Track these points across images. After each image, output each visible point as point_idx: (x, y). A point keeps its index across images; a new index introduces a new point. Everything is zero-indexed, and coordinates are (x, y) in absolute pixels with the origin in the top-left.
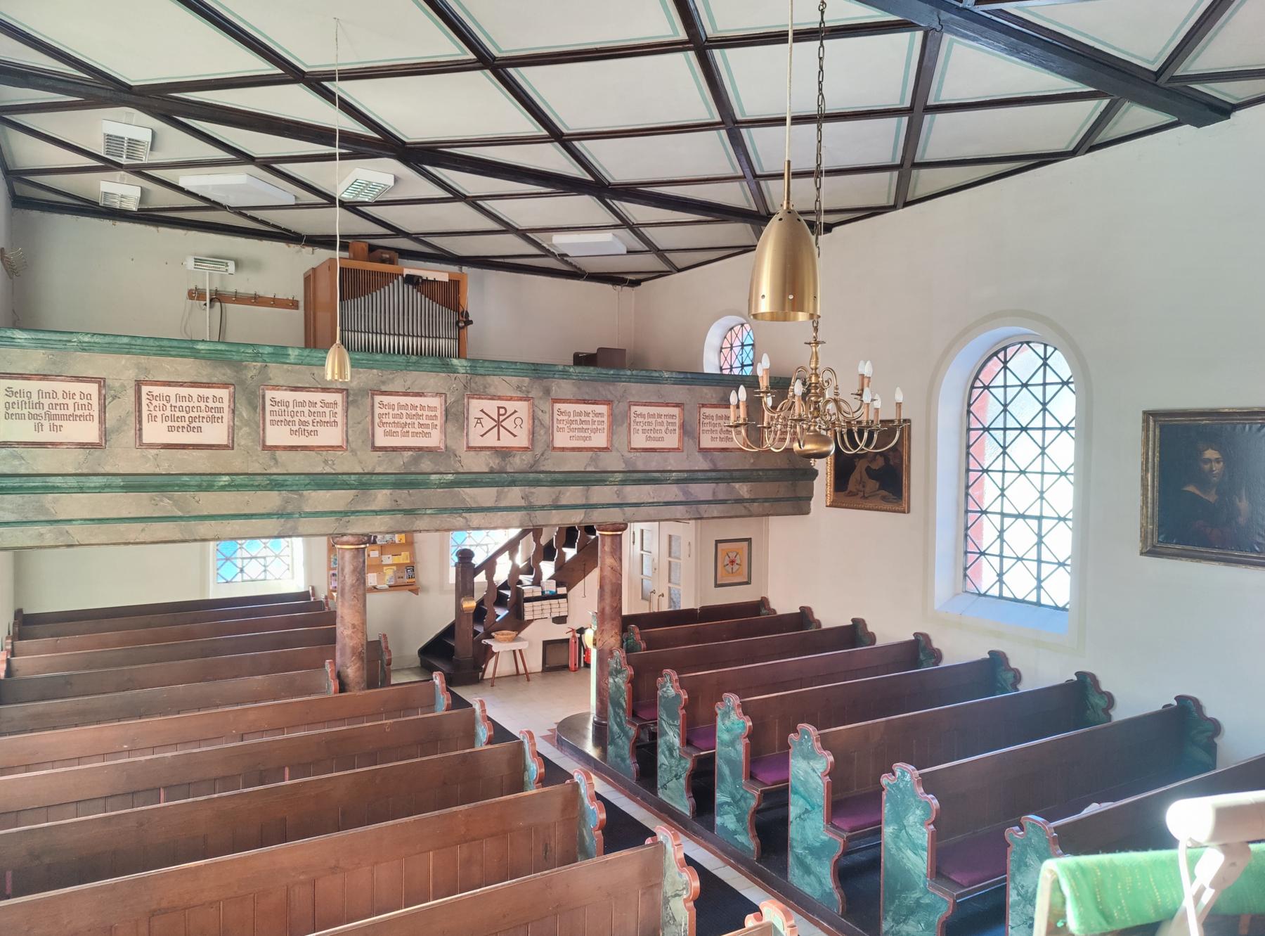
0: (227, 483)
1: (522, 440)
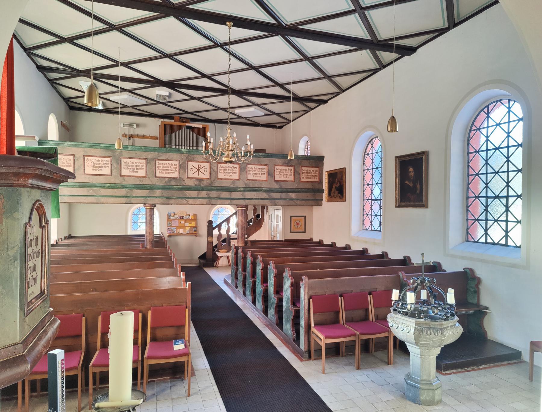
1: (207, 176)
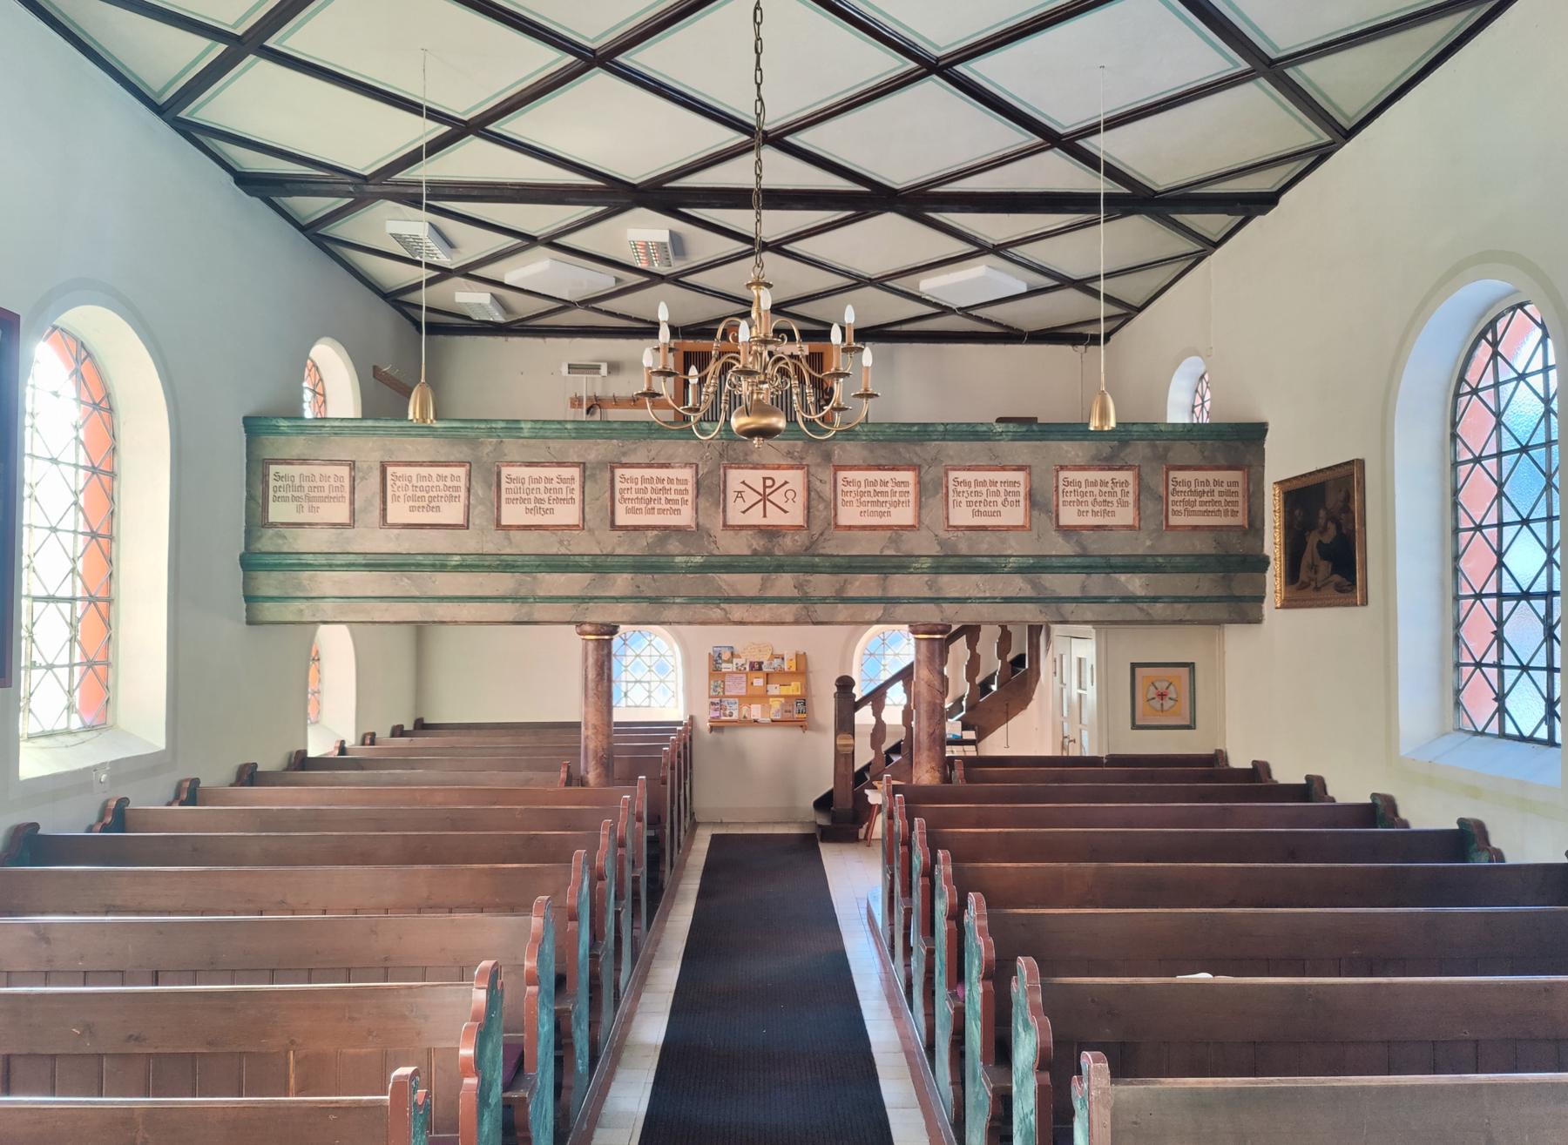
0: (458, 563)
1: (796, 516)
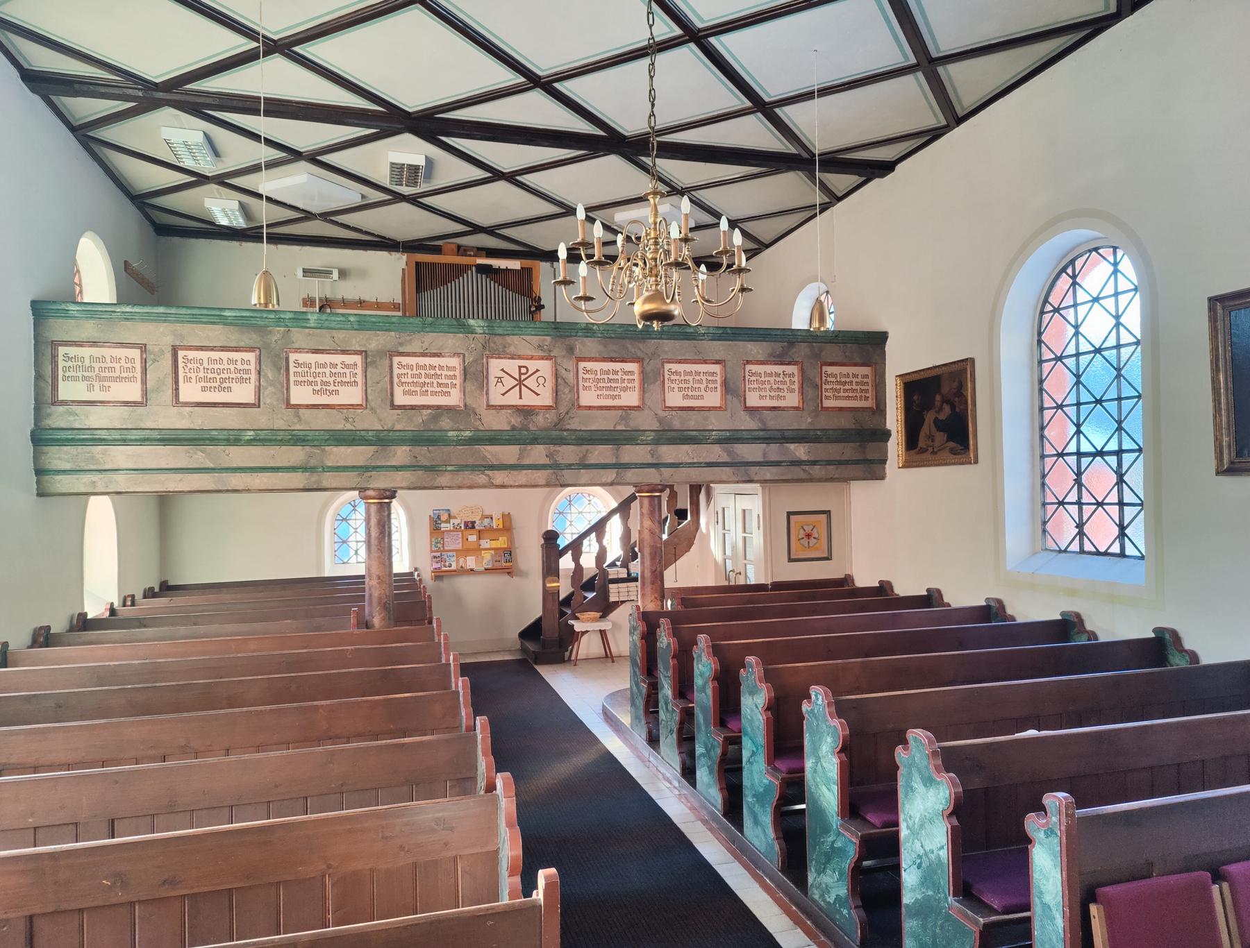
0: (252, 437)
1: (546, 398)
